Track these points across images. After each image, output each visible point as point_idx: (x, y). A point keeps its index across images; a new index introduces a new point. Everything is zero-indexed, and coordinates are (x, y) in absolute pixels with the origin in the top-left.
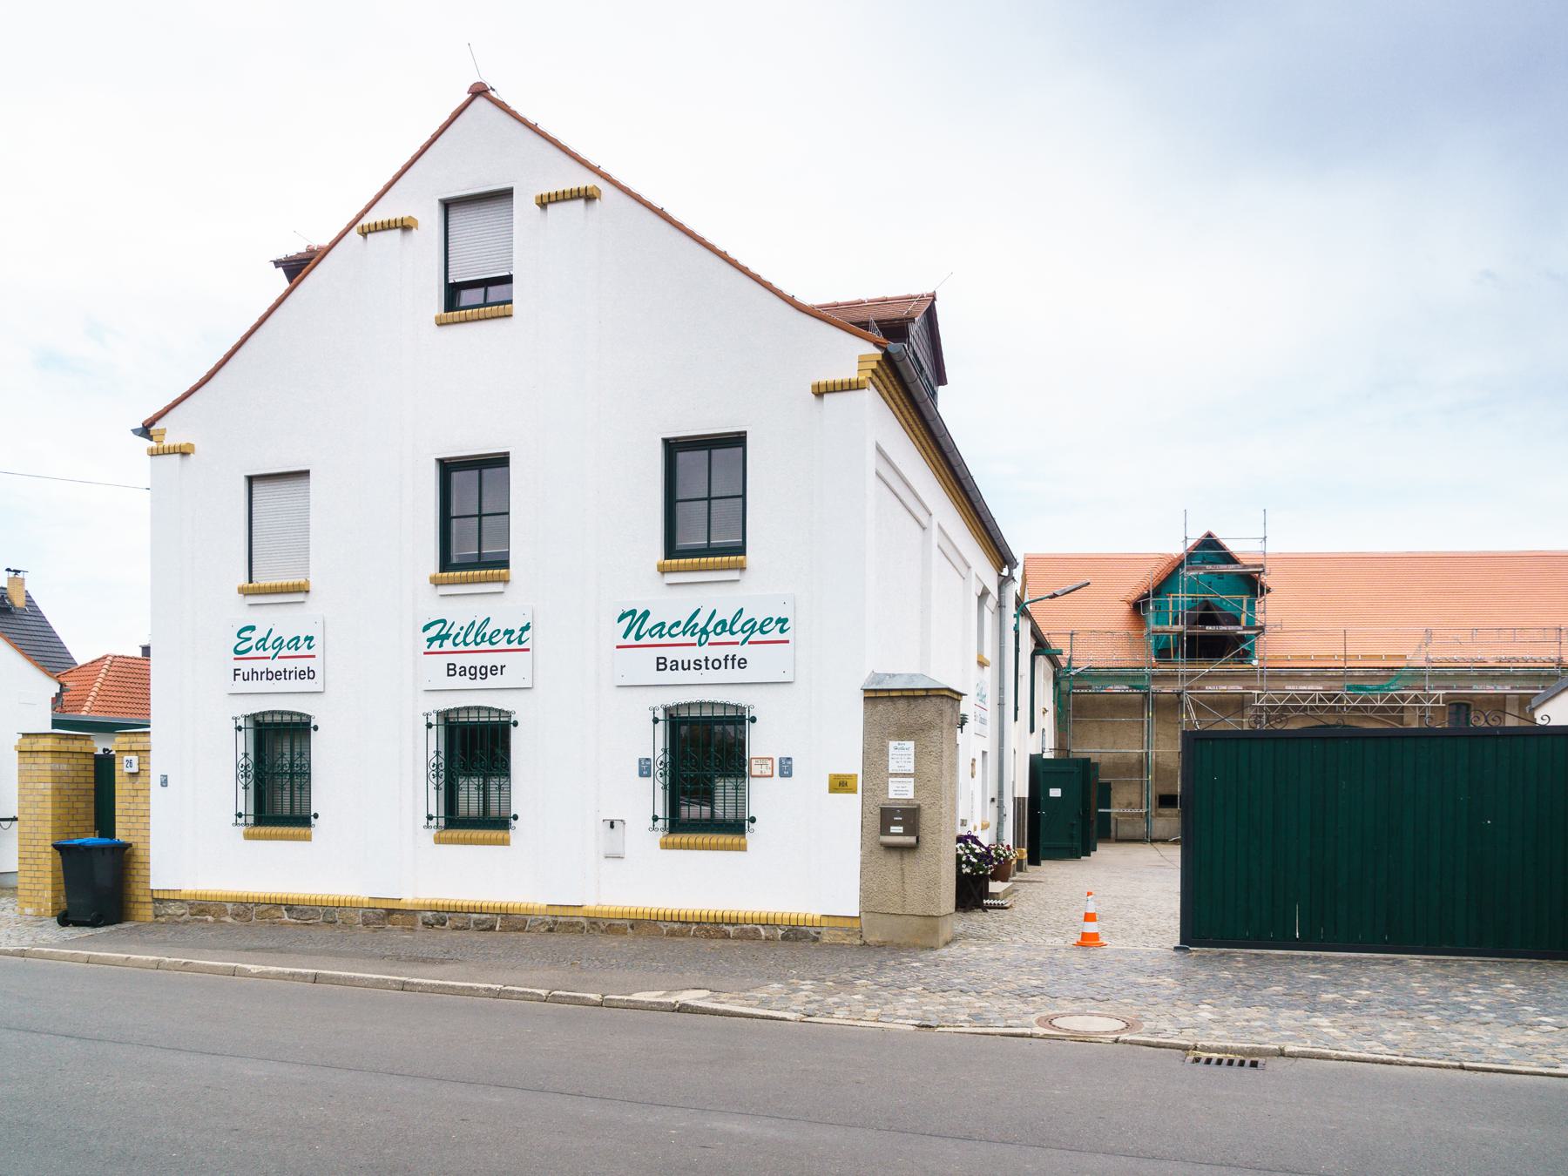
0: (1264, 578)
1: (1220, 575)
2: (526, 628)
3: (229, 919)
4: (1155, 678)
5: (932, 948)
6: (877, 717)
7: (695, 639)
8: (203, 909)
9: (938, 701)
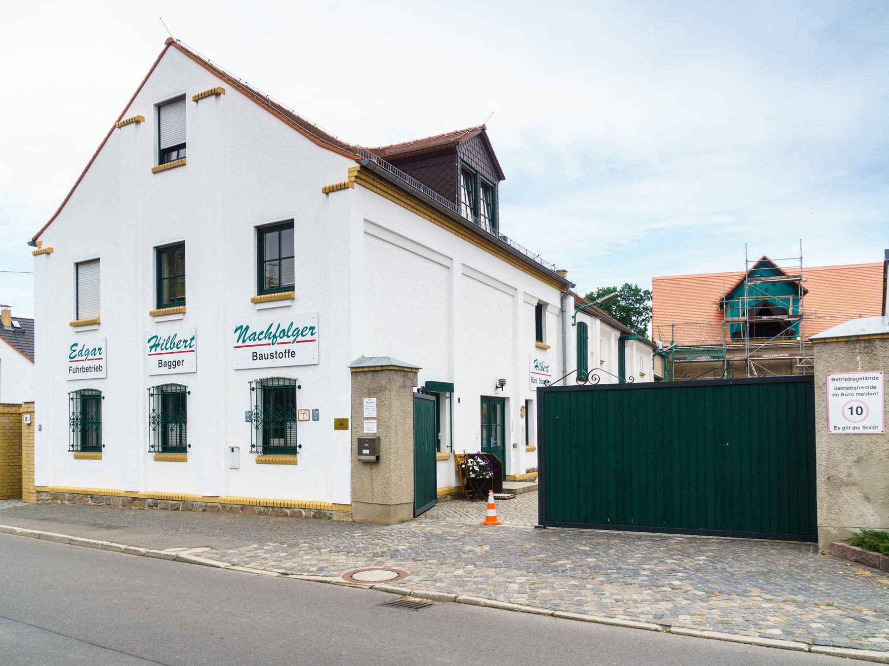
0: (803, 285)
1: (774, 283)
2: (192, 339)
3: (67, 502)
4: (729, 351)
5: (388, 525)
6: (358, 384)
7: (270, 341)
8: (56, 496)
9: (387, 373)
